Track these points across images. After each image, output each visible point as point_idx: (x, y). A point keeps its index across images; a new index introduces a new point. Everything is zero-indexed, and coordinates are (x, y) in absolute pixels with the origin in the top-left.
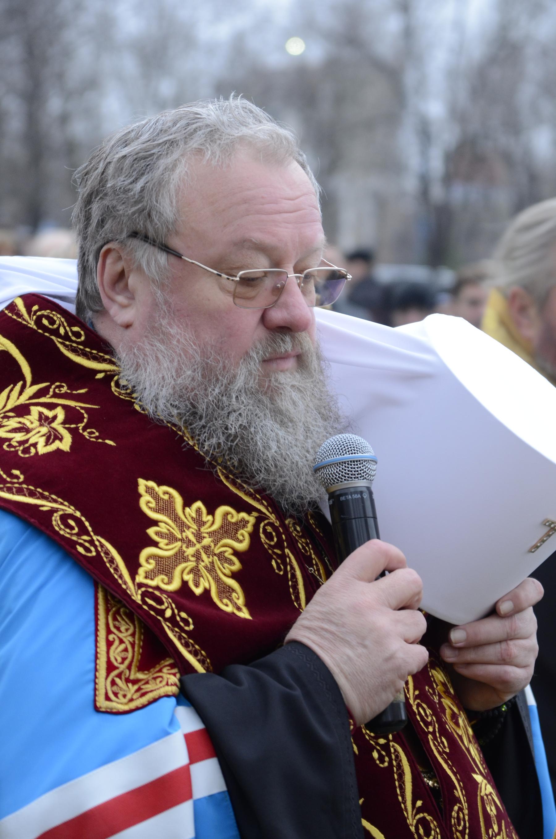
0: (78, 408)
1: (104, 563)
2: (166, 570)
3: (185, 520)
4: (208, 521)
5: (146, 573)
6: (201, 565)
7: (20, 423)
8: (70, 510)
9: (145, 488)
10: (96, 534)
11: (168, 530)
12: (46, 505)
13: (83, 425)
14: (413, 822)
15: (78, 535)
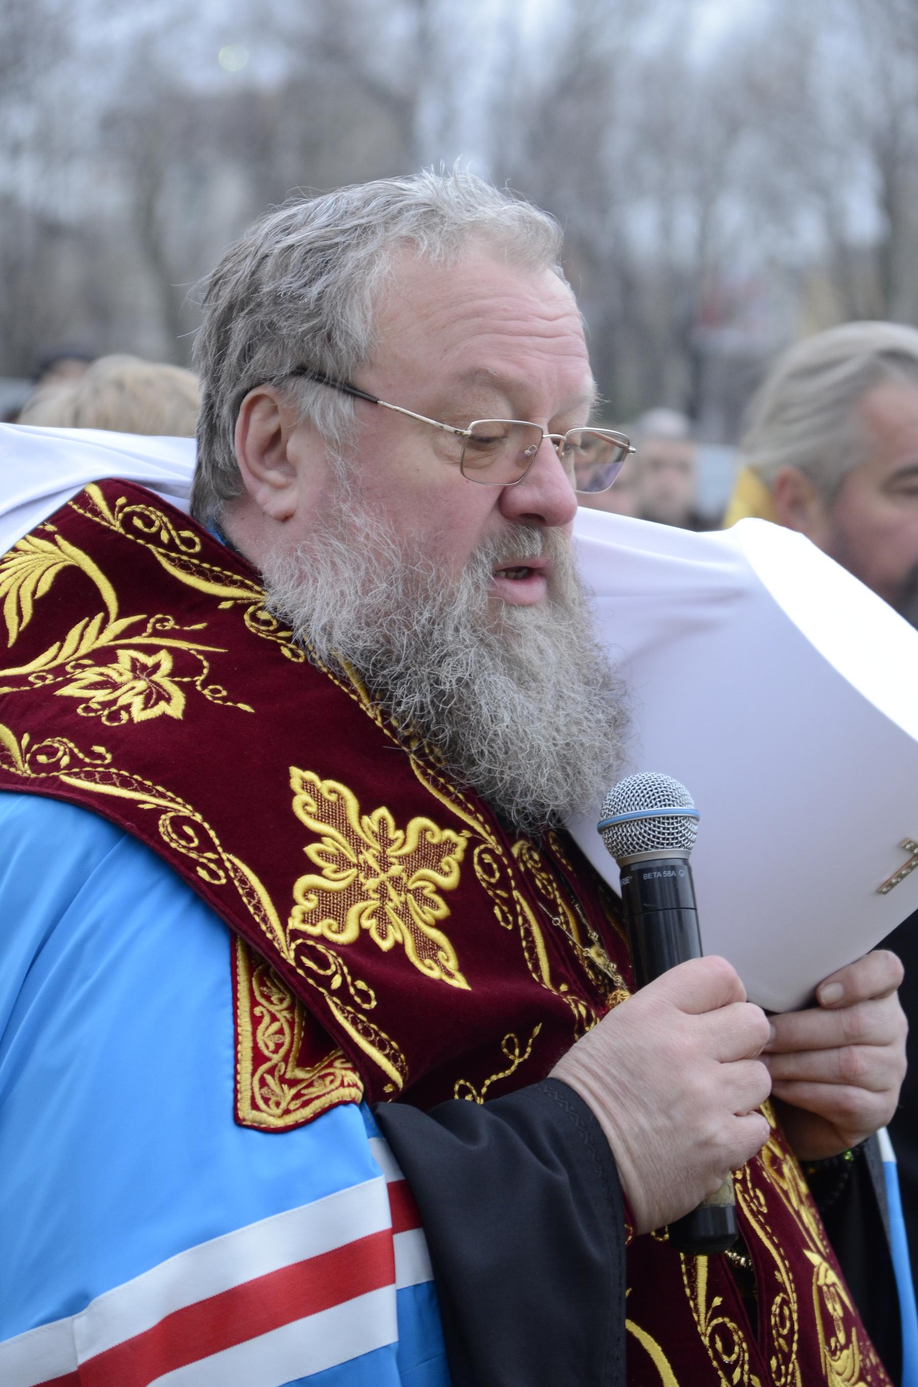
0: (192, 652)
1: (240, 896)
2: (334, 911)
3: (363, 835)
4: (396, 839)
5: (304, 914)
6: (389, 906)
7: (102, 674)
8: (186, 811)
9: (301, 781)
11: (338, 849)
12: (150, 802)
13: (202, 678)
14: (706, 1329)
15: (199, 850)
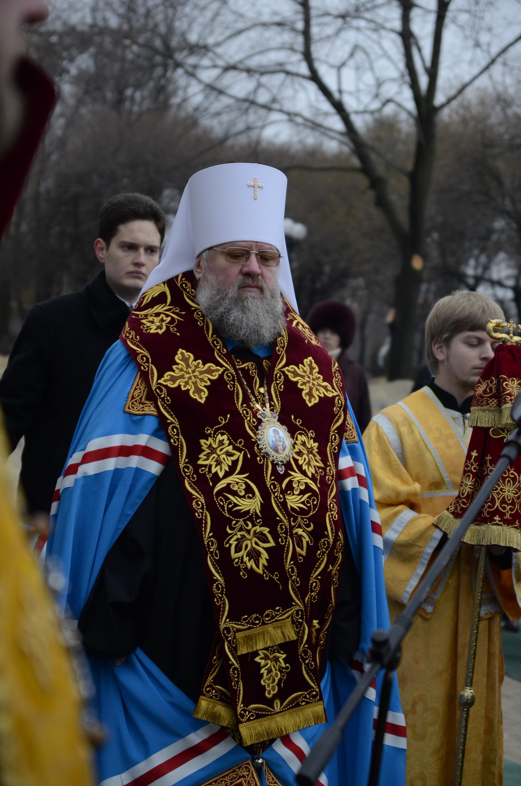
6: (190, 382)
8: (147, 354)
10: (152, 363)
15: (145, 363)
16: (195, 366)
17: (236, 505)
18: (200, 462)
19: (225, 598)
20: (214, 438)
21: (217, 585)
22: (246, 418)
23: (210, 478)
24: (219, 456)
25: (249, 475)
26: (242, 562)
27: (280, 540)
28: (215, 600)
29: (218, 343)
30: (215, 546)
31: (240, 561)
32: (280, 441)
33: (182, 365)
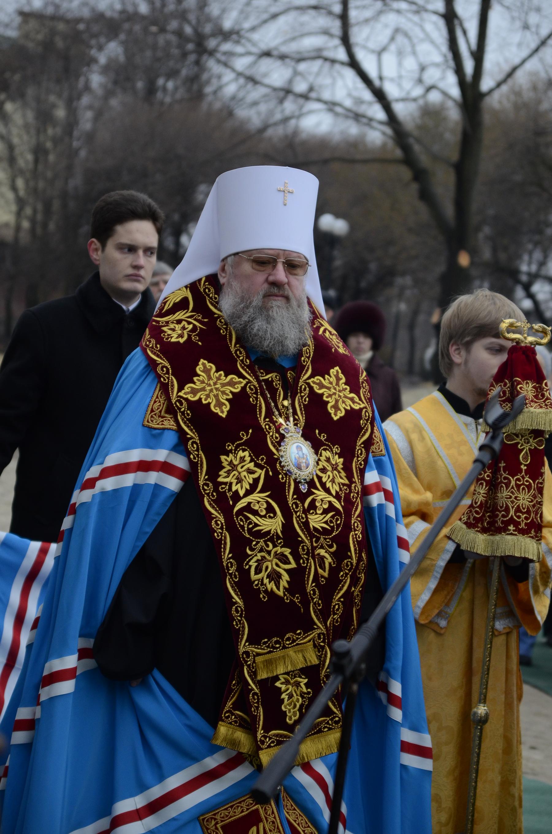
3: (212, 377)
8: (167, 364)
10: (172, 375)
12: (159, 360)
15: (165, 374)
16: (216, 377)
17: (256, 525)
18: (220, 479)
19: (244, 621)
20: (235, 454)
21: (236, 608)
22: (269, 433)
23: (230, 496)
24: (239, 473)
25: (270, 493)
26: (262, 584)
27: (301, 561)
28: (234, 623)
29: (241, 353)
30: (234, 568)
31: (260, 583)
32: (303, 458)
33: (203, 377)
